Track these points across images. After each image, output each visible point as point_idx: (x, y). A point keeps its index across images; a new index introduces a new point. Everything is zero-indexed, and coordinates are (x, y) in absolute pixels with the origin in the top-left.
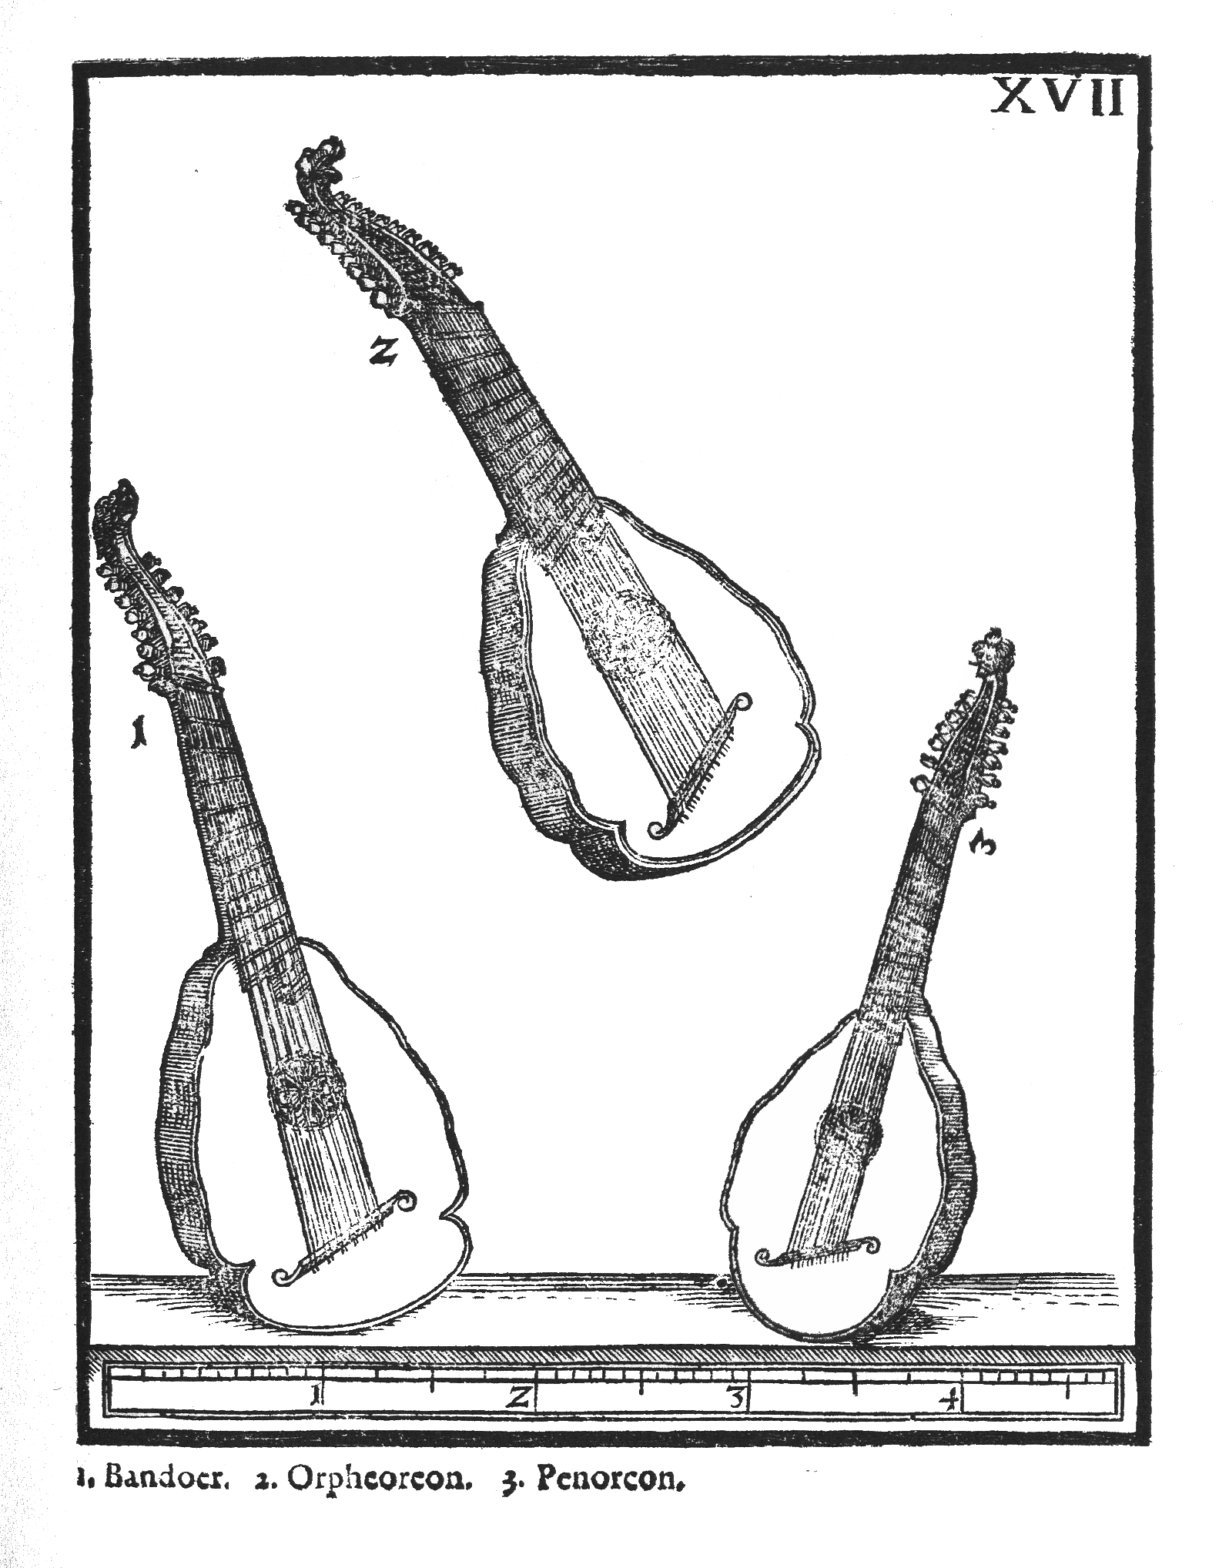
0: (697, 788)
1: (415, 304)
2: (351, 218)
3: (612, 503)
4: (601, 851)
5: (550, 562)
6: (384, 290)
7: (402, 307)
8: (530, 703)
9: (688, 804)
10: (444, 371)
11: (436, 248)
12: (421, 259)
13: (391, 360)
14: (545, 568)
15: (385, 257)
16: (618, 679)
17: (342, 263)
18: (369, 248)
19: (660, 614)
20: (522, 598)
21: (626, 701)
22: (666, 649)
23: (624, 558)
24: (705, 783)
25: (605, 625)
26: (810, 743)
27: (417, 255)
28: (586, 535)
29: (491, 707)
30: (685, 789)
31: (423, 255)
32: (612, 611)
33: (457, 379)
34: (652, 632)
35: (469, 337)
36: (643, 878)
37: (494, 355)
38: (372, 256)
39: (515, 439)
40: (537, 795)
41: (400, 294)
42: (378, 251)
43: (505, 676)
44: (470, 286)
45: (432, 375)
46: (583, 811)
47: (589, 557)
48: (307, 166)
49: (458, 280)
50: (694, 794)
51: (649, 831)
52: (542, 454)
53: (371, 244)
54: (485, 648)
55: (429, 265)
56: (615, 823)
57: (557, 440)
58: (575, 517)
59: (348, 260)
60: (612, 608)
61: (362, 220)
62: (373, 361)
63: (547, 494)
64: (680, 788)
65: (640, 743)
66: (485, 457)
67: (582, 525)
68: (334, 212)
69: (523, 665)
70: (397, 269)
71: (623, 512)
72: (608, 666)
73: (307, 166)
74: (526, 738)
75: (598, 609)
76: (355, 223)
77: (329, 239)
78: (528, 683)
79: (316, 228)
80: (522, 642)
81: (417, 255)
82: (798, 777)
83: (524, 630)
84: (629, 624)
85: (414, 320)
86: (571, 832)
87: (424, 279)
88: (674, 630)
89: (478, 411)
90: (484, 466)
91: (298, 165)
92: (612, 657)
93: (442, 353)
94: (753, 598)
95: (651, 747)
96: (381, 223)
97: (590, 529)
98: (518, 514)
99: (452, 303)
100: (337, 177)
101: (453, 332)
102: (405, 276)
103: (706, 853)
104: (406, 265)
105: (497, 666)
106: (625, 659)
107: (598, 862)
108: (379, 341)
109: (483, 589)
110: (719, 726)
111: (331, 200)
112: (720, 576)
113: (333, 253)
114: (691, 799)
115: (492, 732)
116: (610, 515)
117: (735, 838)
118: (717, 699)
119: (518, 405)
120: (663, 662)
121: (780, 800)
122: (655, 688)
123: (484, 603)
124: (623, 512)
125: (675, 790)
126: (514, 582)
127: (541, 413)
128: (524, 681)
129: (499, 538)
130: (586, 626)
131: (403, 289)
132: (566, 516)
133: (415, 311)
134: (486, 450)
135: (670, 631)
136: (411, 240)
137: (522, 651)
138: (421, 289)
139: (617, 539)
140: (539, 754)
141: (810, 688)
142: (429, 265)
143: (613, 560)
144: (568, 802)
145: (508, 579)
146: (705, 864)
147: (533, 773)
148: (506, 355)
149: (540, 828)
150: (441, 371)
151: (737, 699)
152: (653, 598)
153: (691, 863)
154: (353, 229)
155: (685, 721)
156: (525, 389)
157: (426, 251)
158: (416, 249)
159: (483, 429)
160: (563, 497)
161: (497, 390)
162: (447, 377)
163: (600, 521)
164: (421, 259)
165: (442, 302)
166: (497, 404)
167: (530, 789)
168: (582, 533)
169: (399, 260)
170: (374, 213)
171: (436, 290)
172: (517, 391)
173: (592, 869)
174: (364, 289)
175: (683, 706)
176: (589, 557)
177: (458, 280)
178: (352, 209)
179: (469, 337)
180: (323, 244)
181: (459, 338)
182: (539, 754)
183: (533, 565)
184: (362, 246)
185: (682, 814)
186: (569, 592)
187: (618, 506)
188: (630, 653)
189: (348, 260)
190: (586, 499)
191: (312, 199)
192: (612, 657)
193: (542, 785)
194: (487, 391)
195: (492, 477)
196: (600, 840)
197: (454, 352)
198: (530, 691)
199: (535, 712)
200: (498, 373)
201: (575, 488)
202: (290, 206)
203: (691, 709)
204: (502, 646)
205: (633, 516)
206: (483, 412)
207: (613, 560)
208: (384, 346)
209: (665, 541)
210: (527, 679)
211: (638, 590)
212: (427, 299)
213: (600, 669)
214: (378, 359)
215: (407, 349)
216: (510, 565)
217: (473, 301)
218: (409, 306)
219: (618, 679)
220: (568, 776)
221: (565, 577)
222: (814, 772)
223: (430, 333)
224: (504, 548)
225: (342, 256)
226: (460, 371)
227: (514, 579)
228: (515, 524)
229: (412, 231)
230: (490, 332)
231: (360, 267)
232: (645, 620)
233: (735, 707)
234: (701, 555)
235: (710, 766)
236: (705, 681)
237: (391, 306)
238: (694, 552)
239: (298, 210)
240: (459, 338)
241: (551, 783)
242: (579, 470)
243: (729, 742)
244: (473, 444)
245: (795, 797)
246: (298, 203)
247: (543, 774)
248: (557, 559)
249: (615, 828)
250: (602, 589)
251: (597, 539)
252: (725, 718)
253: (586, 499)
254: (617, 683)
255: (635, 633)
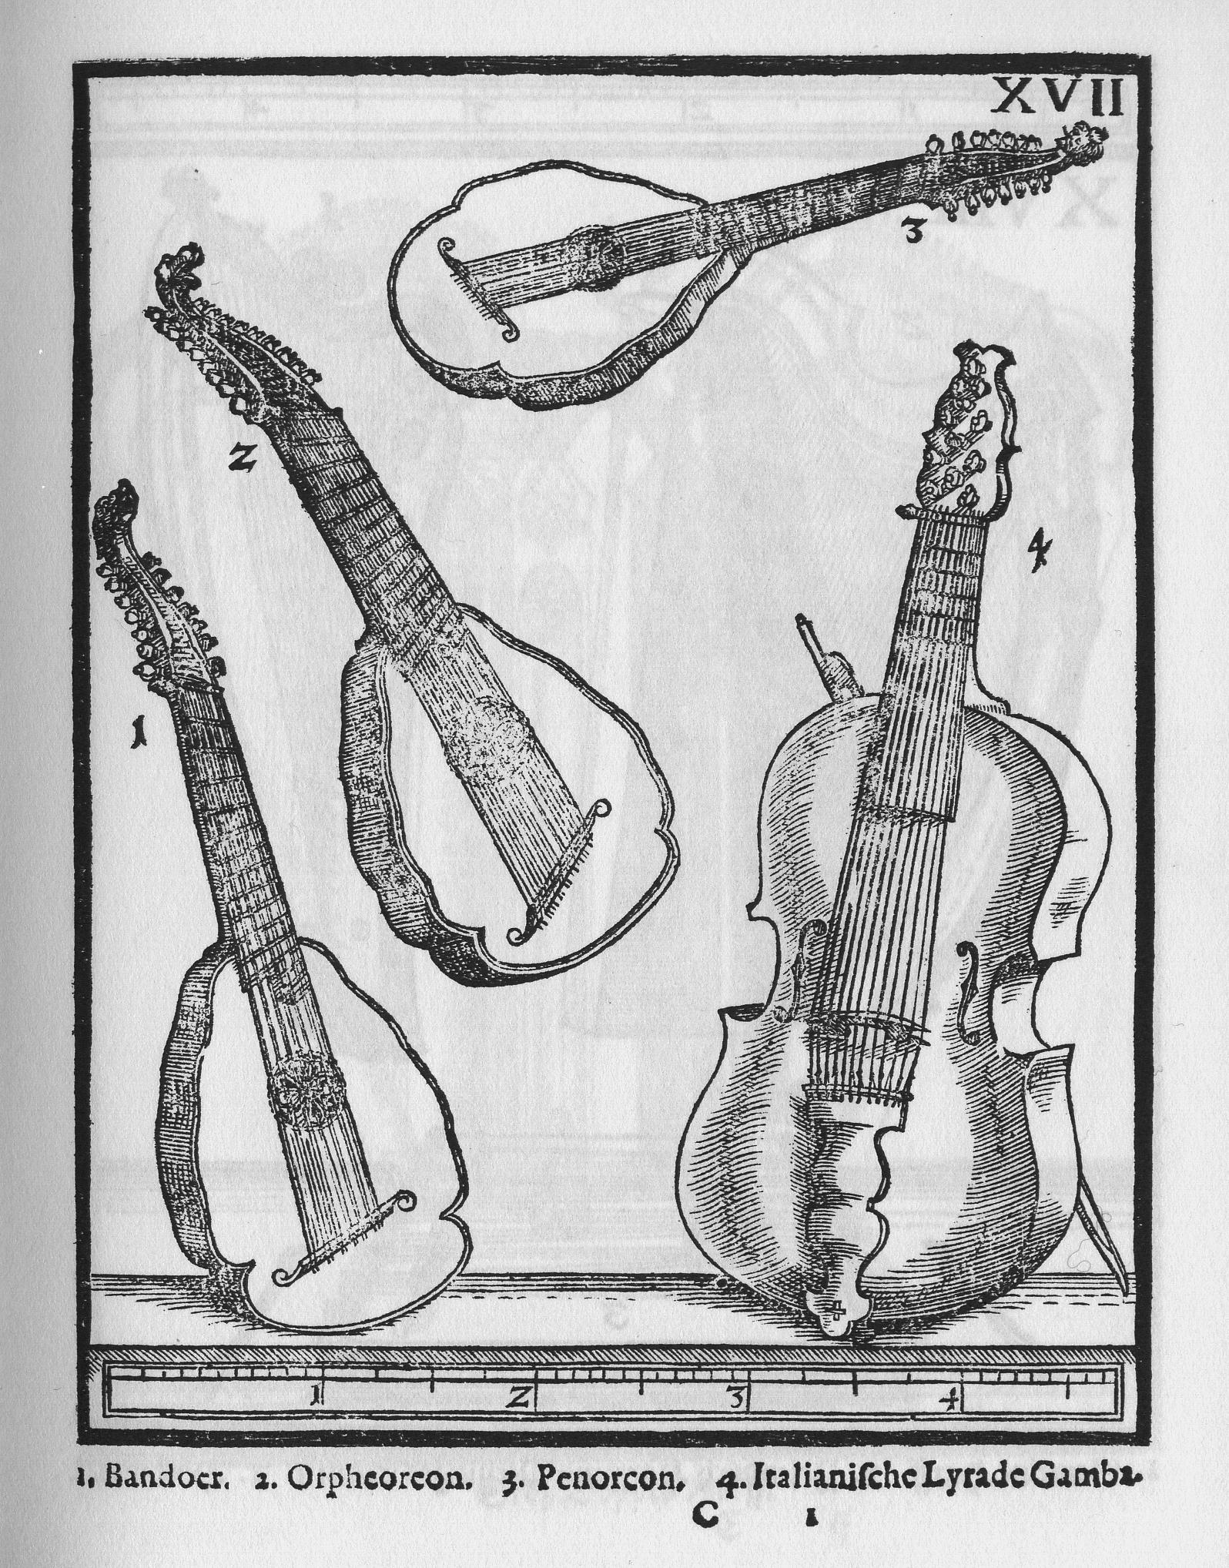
0: (556, 894)
1: (274, 410)
2: (210, 324)
3: (471, 609)
4: (461, 958)
5: (409, 668)
6: (243, 396)
7: (261, 413)
8: (389, 809)
9: (547, 911)
10: (303, 477)
11: (295, 354)
12: (280, 365)
13: (250, 466)
14: (404, 675)
15: (244, 363)
16: (477, 785)
17: (201, 369)
18: (228, 354)
19: (520, 720)
20: (381, 704)
21: (485, 807)
22: (525, 755)
23: (483, 665)
24: (564, 889)
25: (464, 731)
26: (670, 849)
27: (276, 361)
28: (444, 641)
29: (350, 814)
30: (545, 893)
31: (282, 361)
32: (471, 718)
33: (316, 485)
34: (511, 738)
35: (328, 443)
36: (502, 985)
37: (353, 461)
38: (231, 362)
39: (375, 545)
40: (396, 902)
41: (259, 400)
42: (237, 357)
43: (364, 782)
44: (329, 392)
45: (292, 481)
46: (443, 917)
47: (448, 663)
48: (165, 272)
49: (317, 387)
50: (553, 900)
51: (508, 937)
52: (402, 560)
53: (230, 351)
54: (344, 754)
55: (288, 371)
56: (474, 929)
57: (416, 546)
58: (434, 623)
59: (207, 366)
60: (471, 714)
61: (221, 327)
62: (233, 467)
63: (406, 600)
64: (539, 894)
65: (499, 849)
66: (344, 564)
67: (441, 631)
68: (193, 318)
69: (382, 771)
70: (257, 375)
71: (483, 618)
72: (467, 773)
73: (165, 272)
74: (385, 845)
75: (458, 715)
76: (214, 329)
77: (188, 345)
78: (387, 789)
79: (175, 335)
80: (381, 749)
81: (276, 361)
82: (657, 884)
83: (383, 734)
84: (488, 730)
85: (273, 427)
86: (430, 938)
87: (283, 385)
88: (533, 736)
89: (337, 517)
90: (343, 572)
91: (157, 271)
92: (471, 763)
93: (301, 460)
94: (612, 704)
95: (511, 853)
96: (240, 329)
97: (449, 635)
98: (377, 620)
99: (311, 409)
100: (196, 283)
101: (312, 439)
102: (264, 383)
103: (565, 959)
104: (265, 372)
105: (356, 772)
106: (484, 766)
107: (457, 968)
108: (238, 447)
109: (342, 695)
110: (578, 832)
111: (190, 307)
112: (579, 682)
113: (192, 359)
114: (550, 905)
115: (351, 839)
116: (469, 621)
117: (594, 944)
118: (576, 806)
119: (377, 511)
120: (523, 768)
121: (639, 906)
122: (514, 792)
123: (343, 709)
124: (483, 618)
125: (534, 896)
126: (373, 688)
127: (400, 519)
128: (383, 788)
129: (358, 644)
130: (445, 733)
131: (262, 396)
132: (425, 623)
133: (274, 417)
134: (345, 556)
135: (529, 737)
136: (270, 346)
137: (381, 757)
138: (280, 395)
139: (476, 645)
140: (398, 860)
141: (670, 794)
142: (288, 371)
143: (472, 666)
144: (427, 908)
145: (367, 686)
146: (564, 970)
147: (392, 879)
148: (365, 461)
149: (400, 935)
150: (300, 477)
151: (596, 806)
152: (512, 704)
153: (551, 969)
154: (212, 335)
155: (545, 827)
156: (384, 495)
157: (285, 357)
158: (275, 355)
159: (342, 535)
160: (422, 603)
161: (357, 496)
162: (306, 484)
163: (460, 628)
164: (280, 365)
165: (301, 408)
166: (356, 510)
167: (389, 895)
168: (441, 640)
169: (258, 366)
170: (233, 319)
171: (296, 397)
172: (376, 497)
173: (451, 976)
174: (223, 395)
175: (542, 812)
176: (448, 663)
177: (317, 387)
178: (212, 315)
179: (328, 443)
180: (182, 350)
181: (318, 444)
182: (398, 860)
183: (392, 672)
184: (221, 353)
185: (541, 921)
186: (428, 698)
187: (477, 612)
188: (489, 760)
189: (207, 366)
190: (445, 604)
191: (171, 306)
192: (471, 763)
193: (401, 891)
194: (346, 497)
195: (350, 583)
196: (459, 946)
197: (313, 458)
198: (389, 798)
199: (394, 818)
200: (357, 480)
201: (434, 594)
202: (149, 312)
203: (549, 816)
204: (361, 751)
205: (492, 622)
206: (342, 518)
207: (472, 666)
208: (243, 453)
209: (525, 648)
210: (386, 785)
211: (496, 695)
212: (286, 406)
213: (459, 775)
214: (236, 466)
215: (266, 455)
216: (369, 671)
217: (332, 407)
218: (269, 412)
219: (477, 785)
220: (428, 882)
221: (424, 684)
222: (673, 878)
223: (289, 440)
224: (363, 654)
225: (201, 363)
226: (319, 477)
227: (373, 685)
228: (373, 629)
229: (271, 338)
230: (349, 438)
231: (219, 373)
232: (504, 727)
233: (594, 813)
234: (560, 661)
235: (569, 872)
236: (564, 787)
237: (250, 412)
238: (553, 658)
239: (157, 316)
240: (318, 444)
241: (411, 890)
242: (438, 576)
243: (588, 848)
244: (332, 550)
245: (655, 903)
246: (157, 310)
247: (402, 881)
248: (416, 665)
249: (474, 934)
250: (461, 695)
251: (457, 645)
252: (584, 825)
253: (445, 604)
254: (476, 789)
255: (494, 739)
